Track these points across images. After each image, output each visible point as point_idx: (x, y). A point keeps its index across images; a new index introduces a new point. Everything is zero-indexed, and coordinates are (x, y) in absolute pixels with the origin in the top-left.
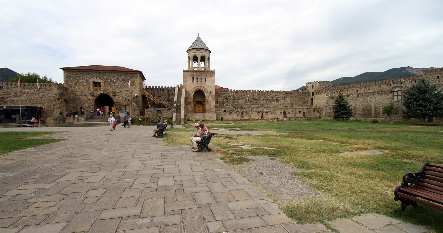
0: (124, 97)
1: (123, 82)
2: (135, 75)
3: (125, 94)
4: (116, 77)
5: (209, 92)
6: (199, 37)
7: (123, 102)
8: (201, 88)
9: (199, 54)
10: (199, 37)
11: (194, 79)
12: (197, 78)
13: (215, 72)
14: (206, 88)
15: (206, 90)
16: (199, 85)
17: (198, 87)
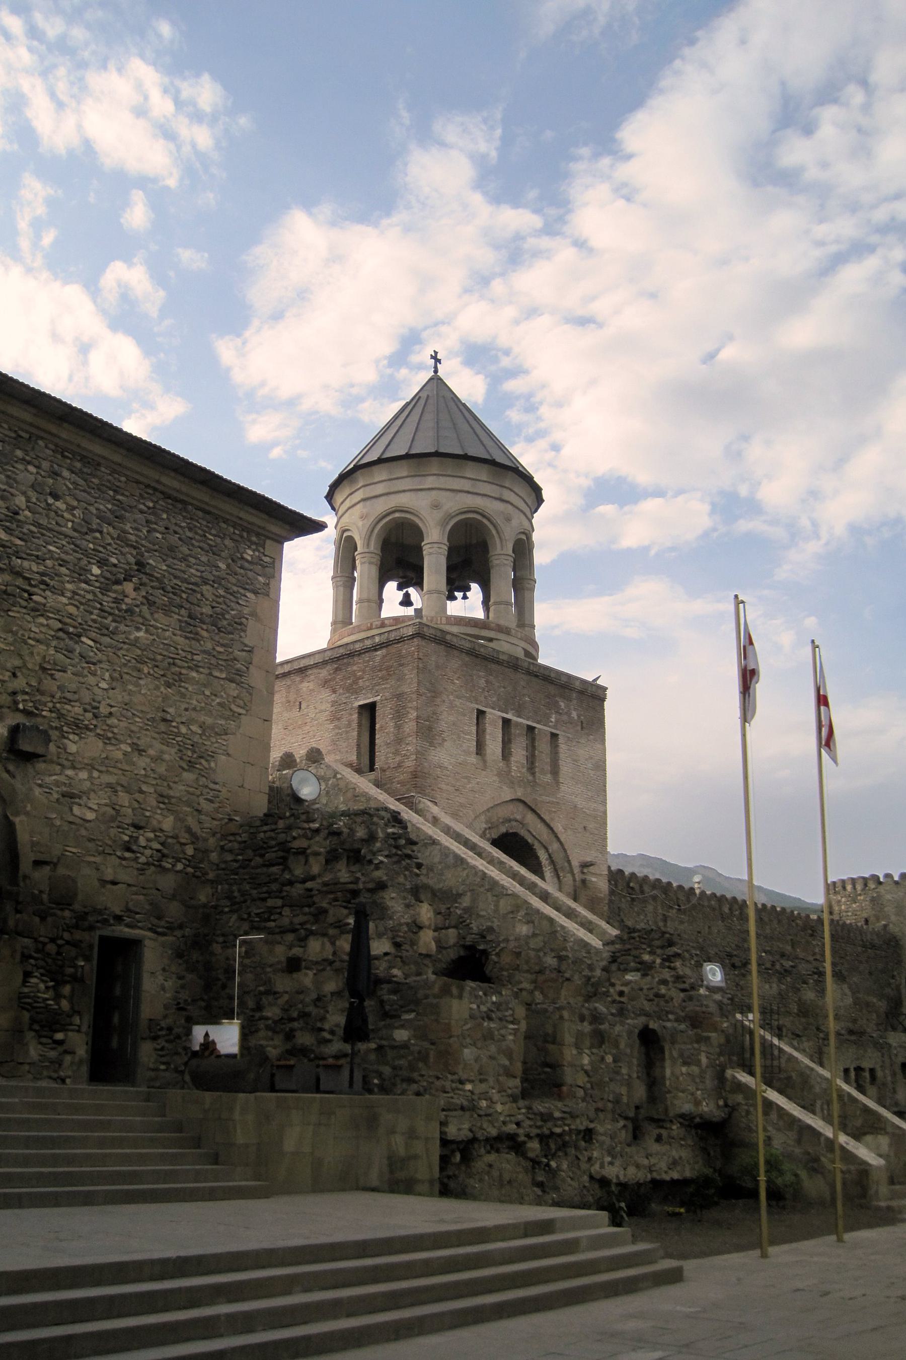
0: (124, 798)
1: (128, 587)
2: (249, 554)
3: (142, 762)
4: (71, 509)
5: (575, 863)
6: (436, 381)
7: (109, 874)
8: (530, 818)
9: (508, 519)
10: (436, 381)
11: (489, 729)
12: (506, 722)
13: (602, 699)
14: (558, 827)
15: (555, 846)
16: (519, 794)
17: (511, 807)
